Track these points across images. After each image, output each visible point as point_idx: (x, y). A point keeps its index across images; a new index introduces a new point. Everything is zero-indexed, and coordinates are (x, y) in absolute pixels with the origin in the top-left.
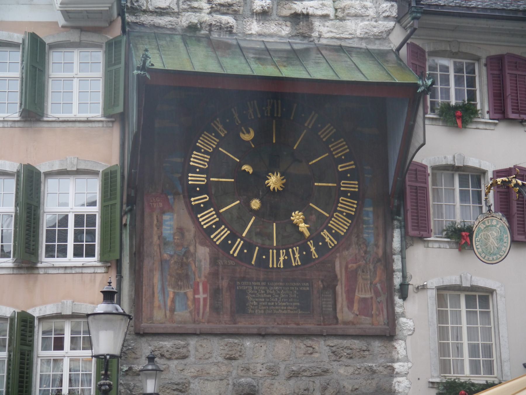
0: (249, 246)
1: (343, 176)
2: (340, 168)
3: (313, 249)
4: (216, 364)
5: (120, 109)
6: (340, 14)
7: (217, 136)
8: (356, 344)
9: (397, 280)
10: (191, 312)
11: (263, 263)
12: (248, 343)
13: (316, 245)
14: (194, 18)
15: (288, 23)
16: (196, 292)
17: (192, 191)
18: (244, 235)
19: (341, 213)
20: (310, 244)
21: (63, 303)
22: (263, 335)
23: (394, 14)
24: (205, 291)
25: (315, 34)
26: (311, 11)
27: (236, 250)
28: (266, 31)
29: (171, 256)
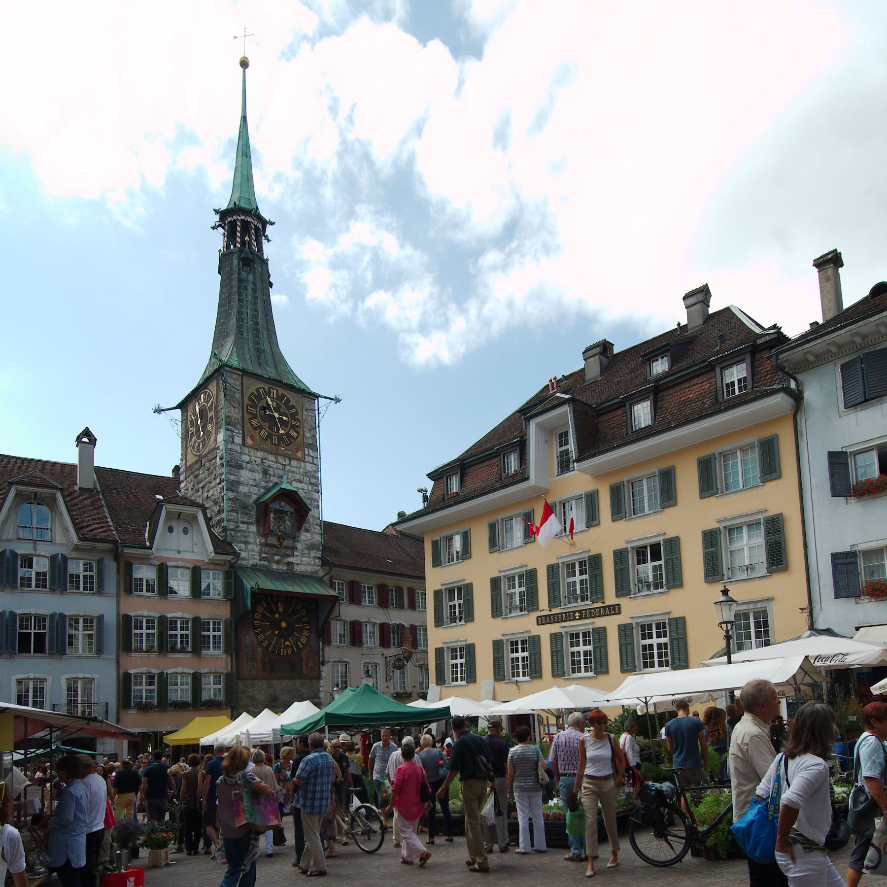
0: (274, 647)
1: (304, 623)
2: (304, 620)
5: (233, 597)
7: (264, 607)
11: (279, 654)
14: (254, 562)
16: (257, 664)
17: (255, 627)
20: (294, 647)
25: (295, 570)
26: (294, 561)
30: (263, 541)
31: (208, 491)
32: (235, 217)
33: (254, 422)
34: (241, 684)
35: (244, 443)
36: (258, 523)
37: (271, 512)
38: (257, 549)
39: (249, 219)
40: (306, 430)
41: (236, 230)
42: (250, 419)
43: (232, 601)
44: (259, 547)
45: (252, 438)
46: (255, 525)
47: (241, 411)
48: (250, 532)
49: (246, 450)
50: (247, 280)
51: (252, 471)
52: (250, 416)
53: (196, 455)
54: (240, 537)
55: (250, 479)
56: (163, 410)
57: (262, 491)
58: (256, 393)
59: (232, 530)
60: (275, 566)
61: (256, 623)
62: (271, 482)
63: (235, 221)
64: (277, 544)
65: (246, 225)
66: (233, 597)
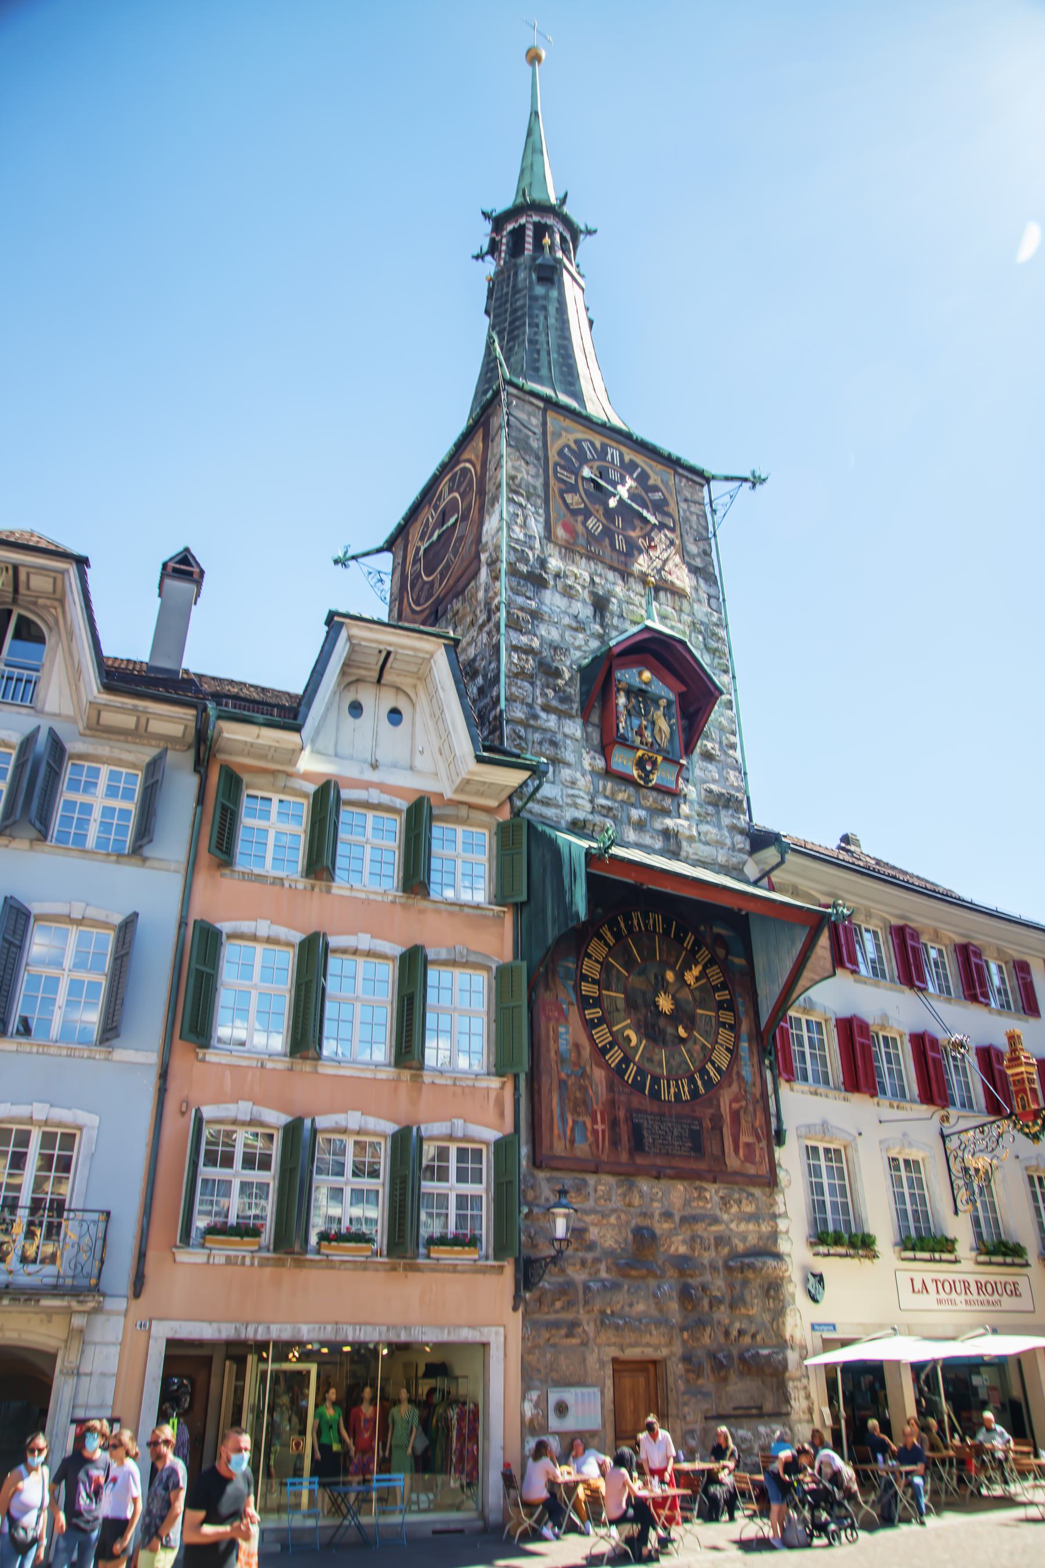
0: (640, 1071)
1: (720, 1006)
3: (699, 1083)
4: (614, 1211)
5: (524, 898)
6: (702, 838)
7: (606, 944)
9: (774, 1126)
10: (590, 1146)
11: (655, 1095)
13: (702, 1079)
15: (661, 838)
16: (594, 1121)
18: (637, 1059)
19: (722, 1045)
20: (697, 1076)
21: (453, 1124)
23: (748, 847)
24: (603, 1122)
27: (630, 1075)
28: (641, 841)
29: (568, 1076)
32: (523, 221)
35: (549, 535)
37: (618, 690)
38: (584, 782)
39: (550, 221)
41: (523, 241)
42: (562, 493)
43: (518, 908)
44: (589, 778)
45: (569, 529)
46: (579, 721)
47: (541, 471)
48: (566, 736)
50: (546, 297)
51: (568, 593)
52: (563, 486)
53: (422, 611)
54: (540, 743)
55: (565, 612)
56: (354, 558)
58: (574, 446)
59: (520, 722)
61: (587, 989)
63: (522, 227)
64: (635, 773)
66: (524, 898)
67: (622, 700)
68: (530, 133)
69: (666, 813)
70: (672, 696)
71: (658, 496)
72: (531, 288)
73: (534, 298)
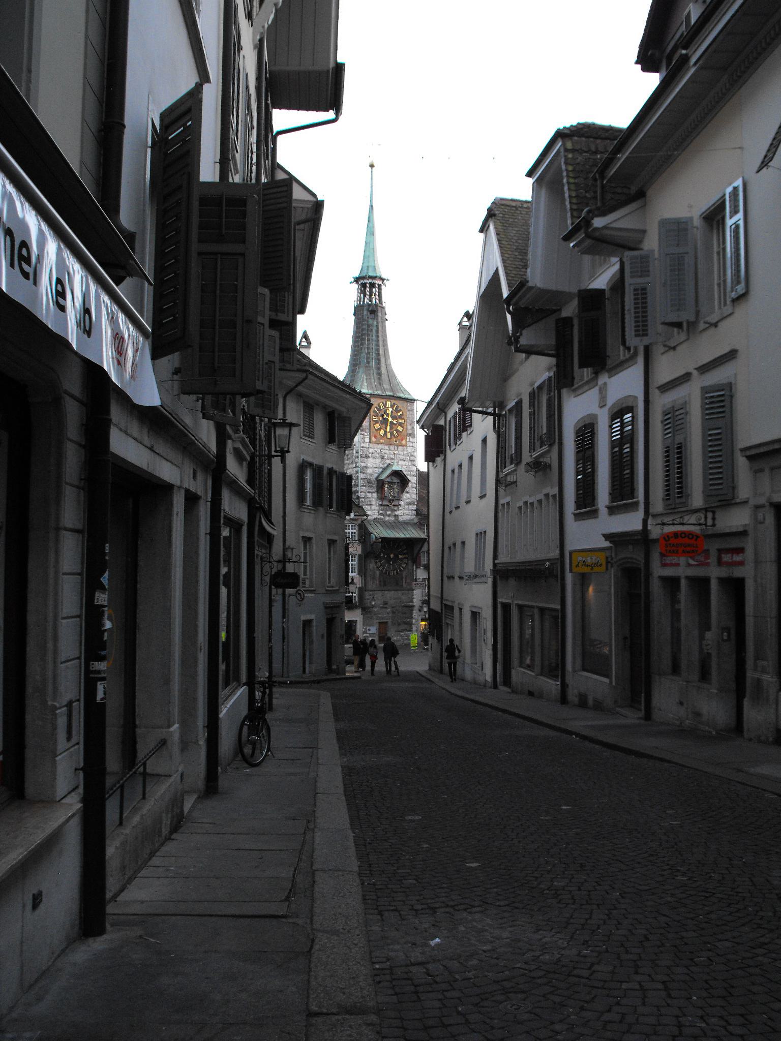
0: (386, 570)
1: (405, 554)
2: (405, 552)
8: (406, 592)
11: (389, 575)
12: (386, 592)
14: (374, 517)
22: (389, 590)
30: (381, 503)
31: (347, 469)
33: (377, 426)
34: (367, 593)
36: (377, 492)
40: (408, 425)
45: (375, 437)
49: (371, 445)
50: (372, 325)
57: (381, 470)
60: (387, 518)
62: (386, 463)
63: (366, 283)
65: (372, 285)
67: (386, 486)
68: (369, 221)
69: (396, 510)
70: (399, 481)
71: (401, 413)
72: (368, 321)
73: (369, 326)
